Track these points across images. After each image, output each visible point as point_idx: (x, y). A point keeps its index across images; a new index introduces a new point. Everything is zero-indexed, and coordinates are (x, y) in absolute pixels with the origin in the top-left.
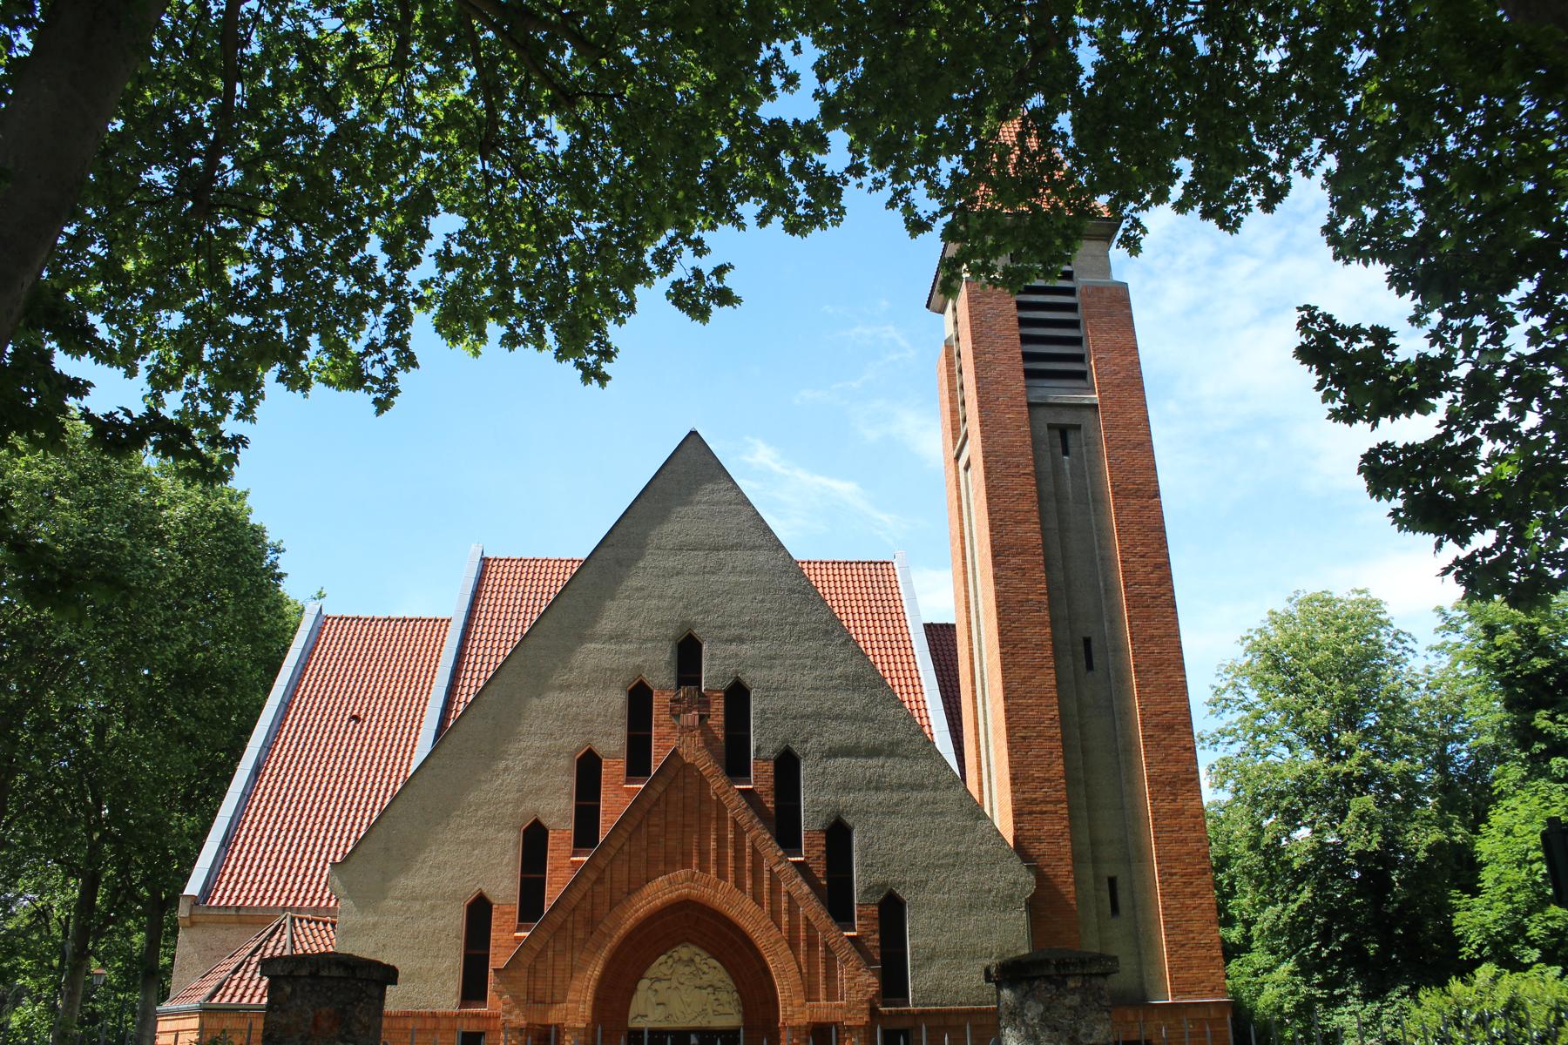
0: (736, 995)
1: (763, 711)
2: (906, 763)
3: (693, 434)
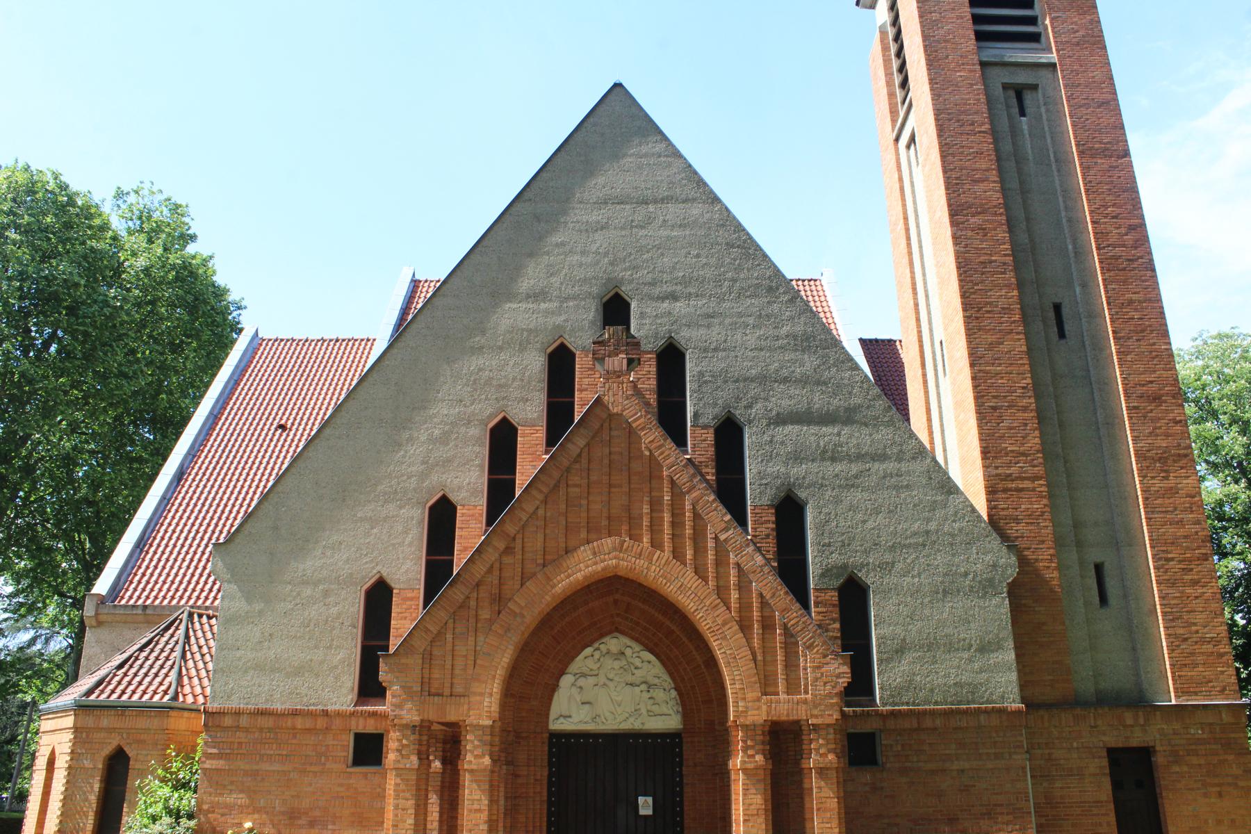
0: (674, 693)
1: (701, 374)
2: (865, 431)
3: (618, 86)
